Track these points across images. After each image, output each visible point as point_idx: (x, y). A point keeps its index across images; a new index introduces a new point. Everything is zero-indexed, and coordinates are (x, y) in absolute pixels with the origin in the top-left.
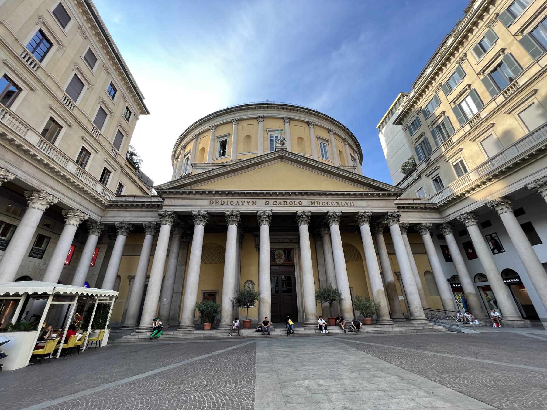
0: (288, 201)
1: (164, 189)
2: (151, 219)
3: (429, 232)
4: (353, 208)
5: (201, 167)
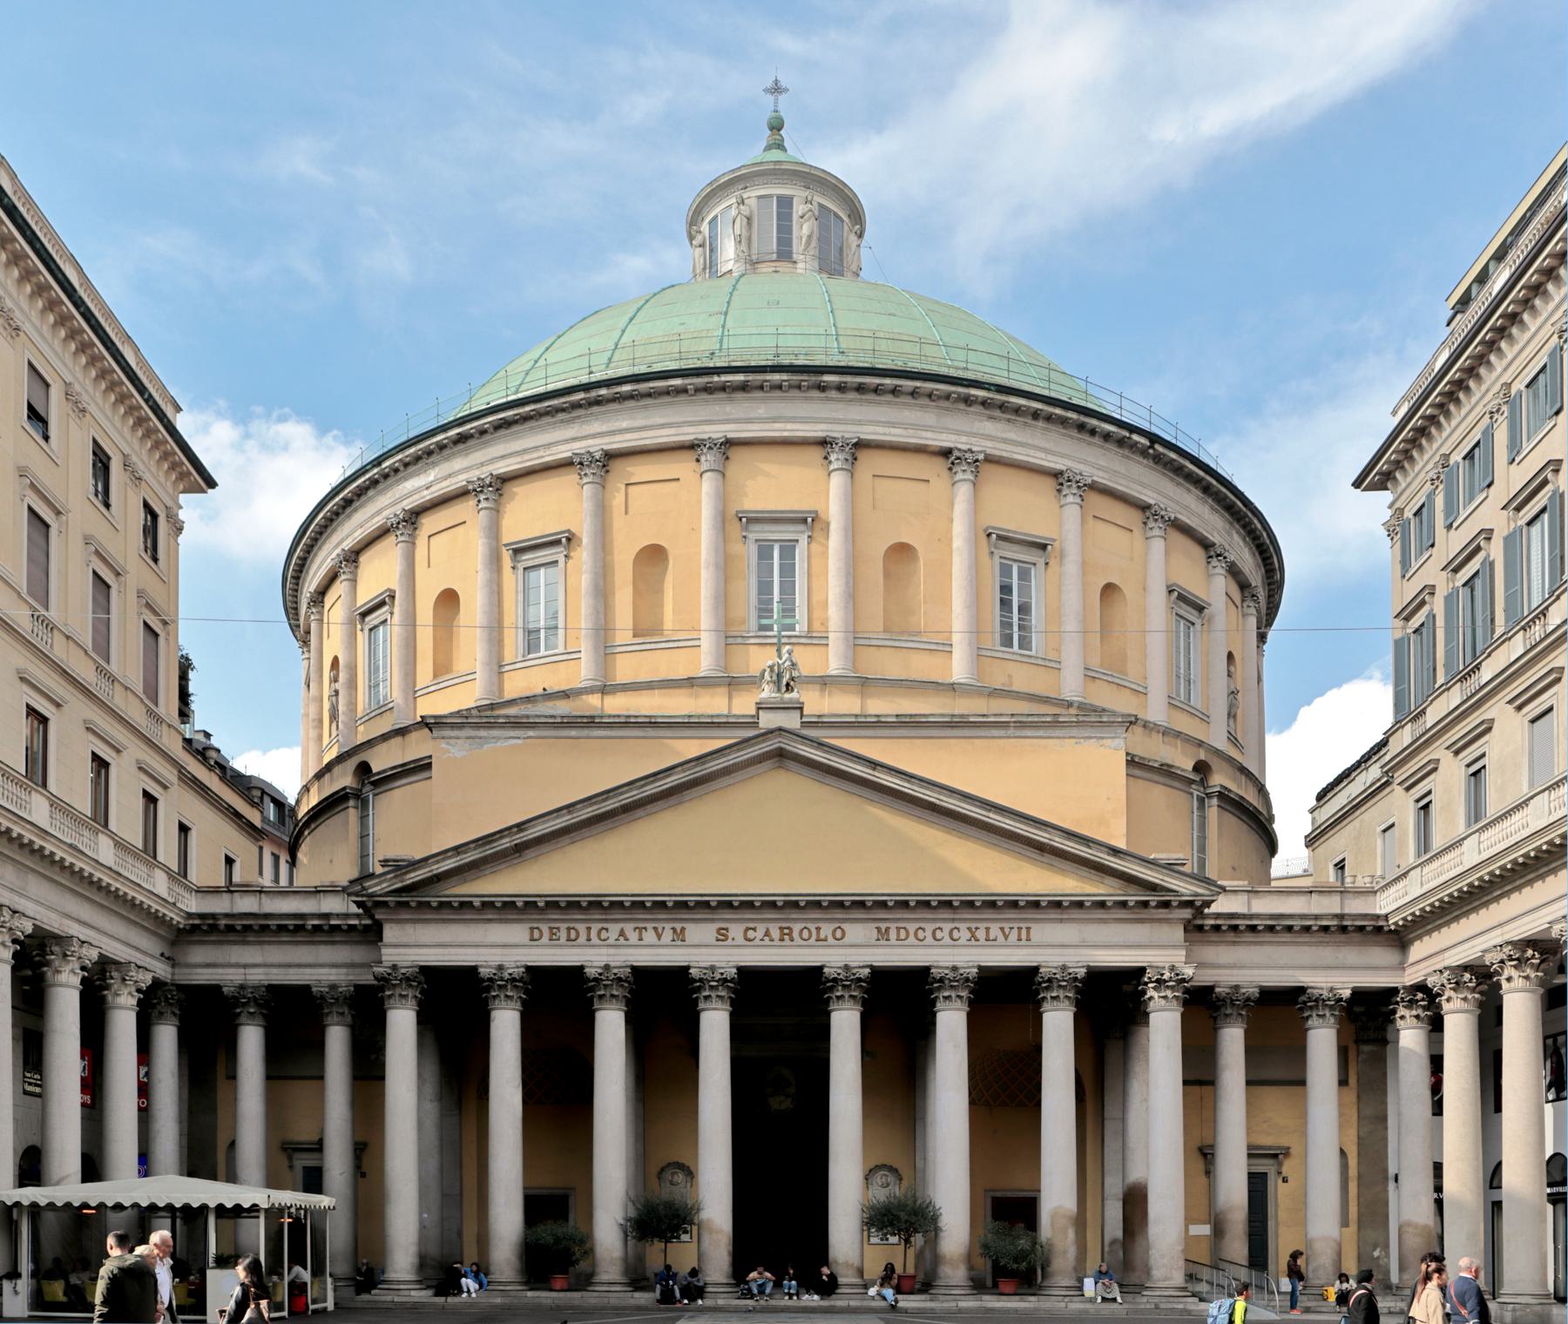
0: (797, 927)
1: (380, 896)
3: (1332, 1020)
4: (1025, 951)
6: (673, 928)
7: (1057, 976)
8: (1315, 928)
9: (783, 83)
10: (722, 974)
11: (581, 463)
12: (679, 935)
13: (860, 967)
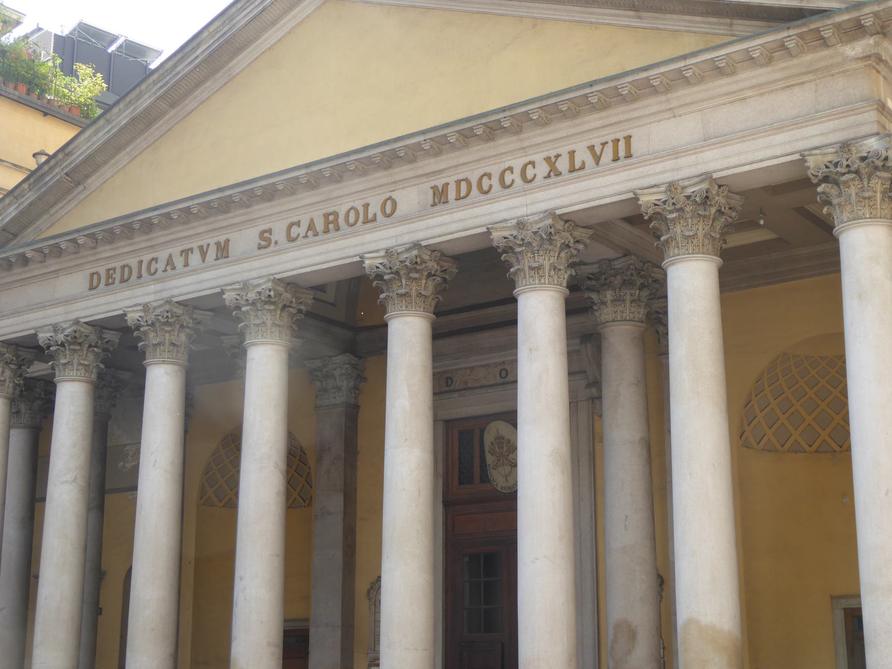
12: (223, 250)
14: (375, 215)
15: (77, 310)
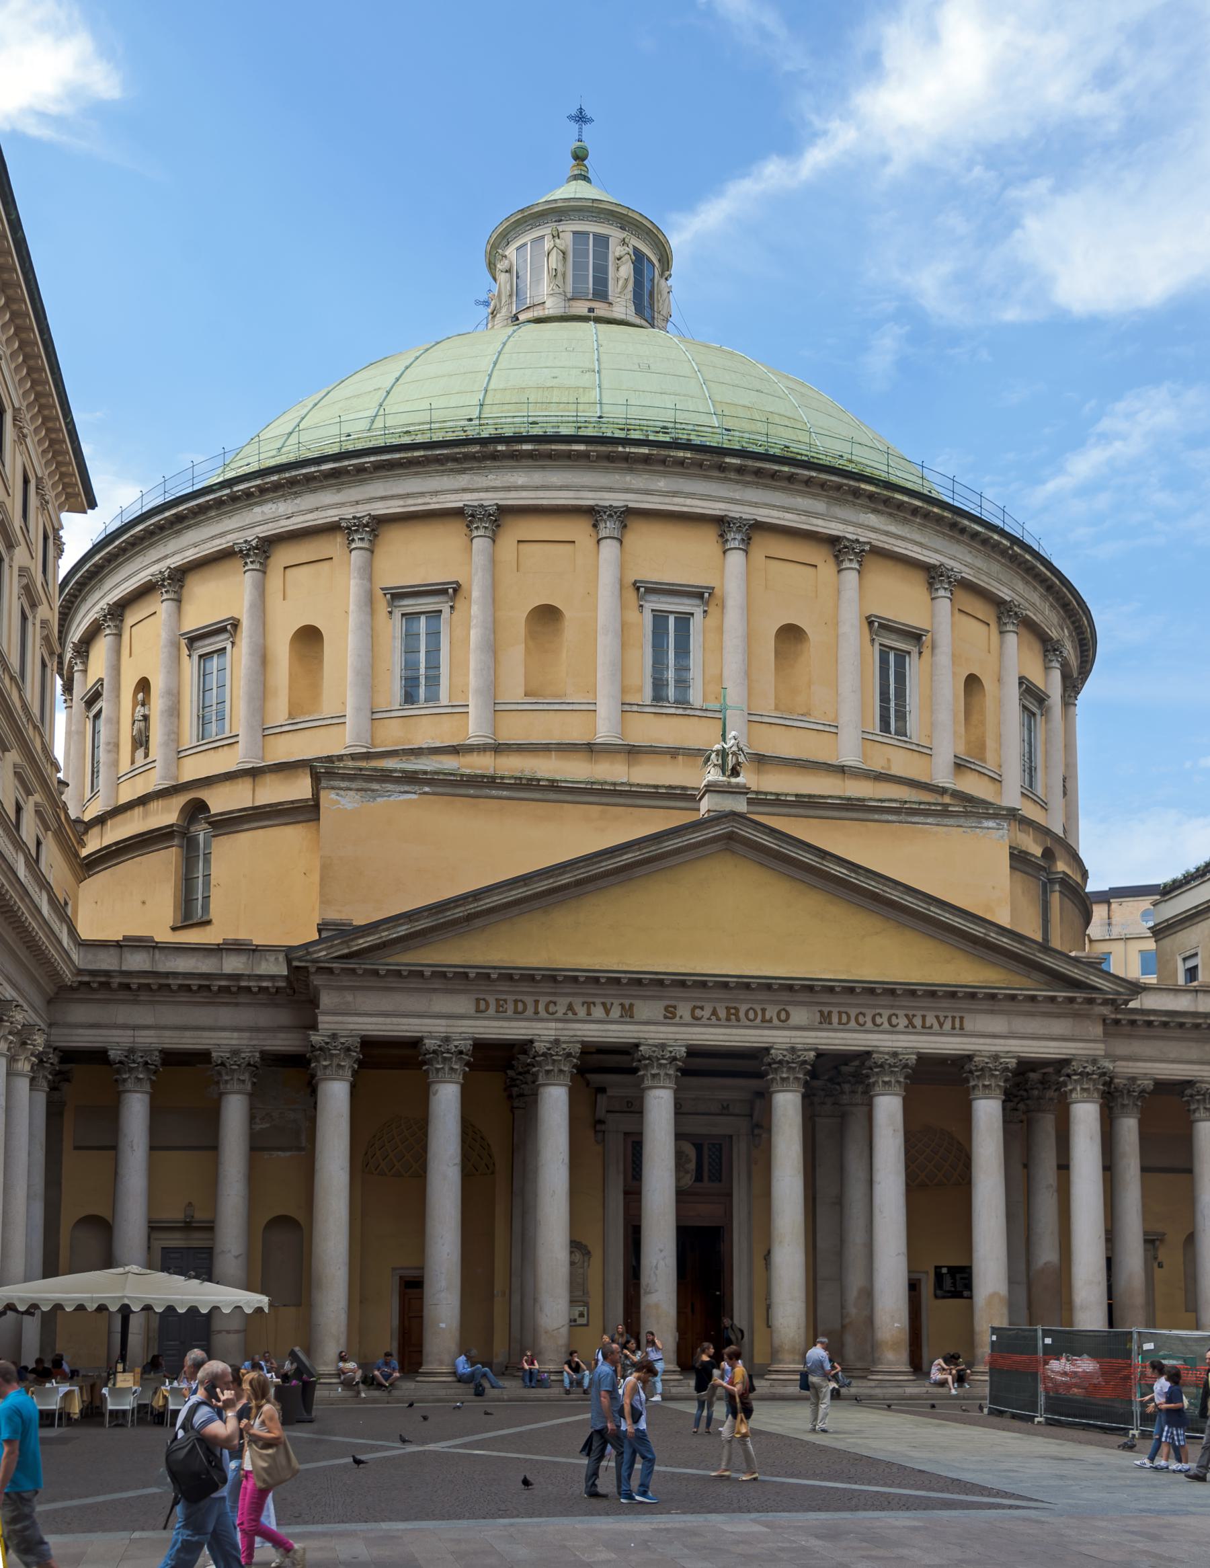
2: (235, 1035)
4: (958, 1040)
5: (354, 785)
6: (621, 1004)
7: (990, 1065)
8: (1204, 1026)
9: (588, 113)
10: (671, 1052)
11: (472, 516)
13: (805, 1050)
14: (771, 1018)
15: (462, 1026)
